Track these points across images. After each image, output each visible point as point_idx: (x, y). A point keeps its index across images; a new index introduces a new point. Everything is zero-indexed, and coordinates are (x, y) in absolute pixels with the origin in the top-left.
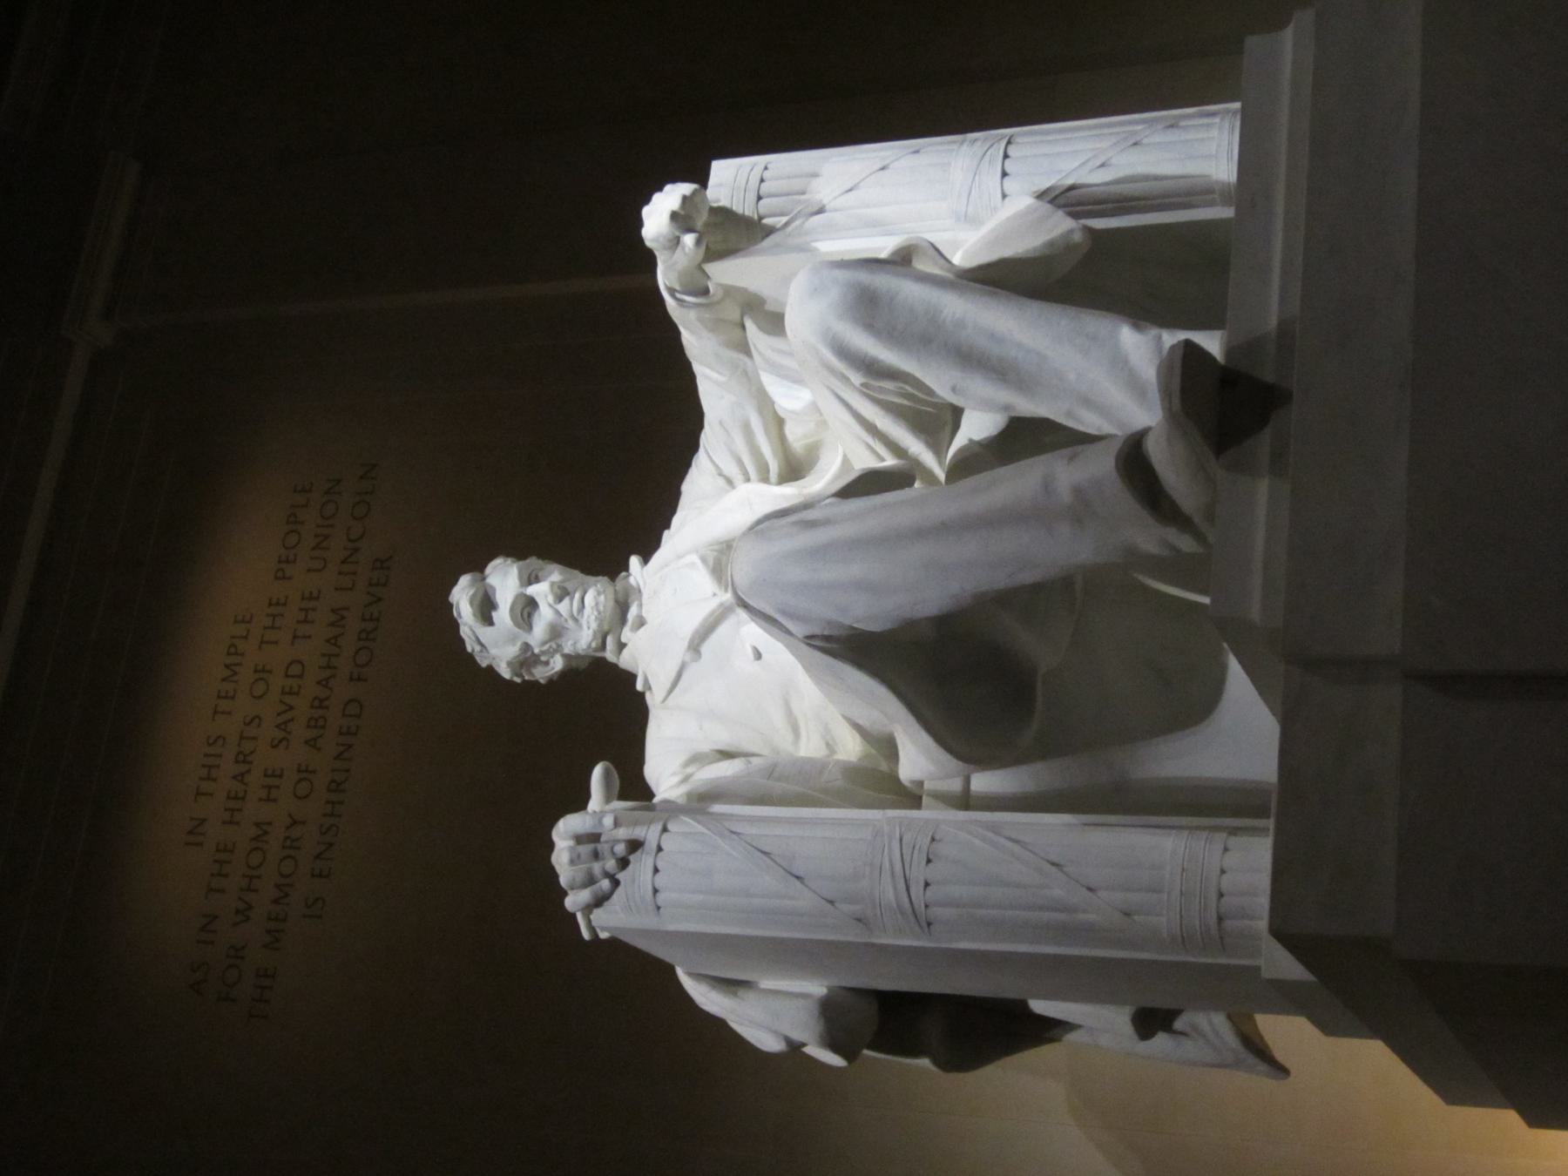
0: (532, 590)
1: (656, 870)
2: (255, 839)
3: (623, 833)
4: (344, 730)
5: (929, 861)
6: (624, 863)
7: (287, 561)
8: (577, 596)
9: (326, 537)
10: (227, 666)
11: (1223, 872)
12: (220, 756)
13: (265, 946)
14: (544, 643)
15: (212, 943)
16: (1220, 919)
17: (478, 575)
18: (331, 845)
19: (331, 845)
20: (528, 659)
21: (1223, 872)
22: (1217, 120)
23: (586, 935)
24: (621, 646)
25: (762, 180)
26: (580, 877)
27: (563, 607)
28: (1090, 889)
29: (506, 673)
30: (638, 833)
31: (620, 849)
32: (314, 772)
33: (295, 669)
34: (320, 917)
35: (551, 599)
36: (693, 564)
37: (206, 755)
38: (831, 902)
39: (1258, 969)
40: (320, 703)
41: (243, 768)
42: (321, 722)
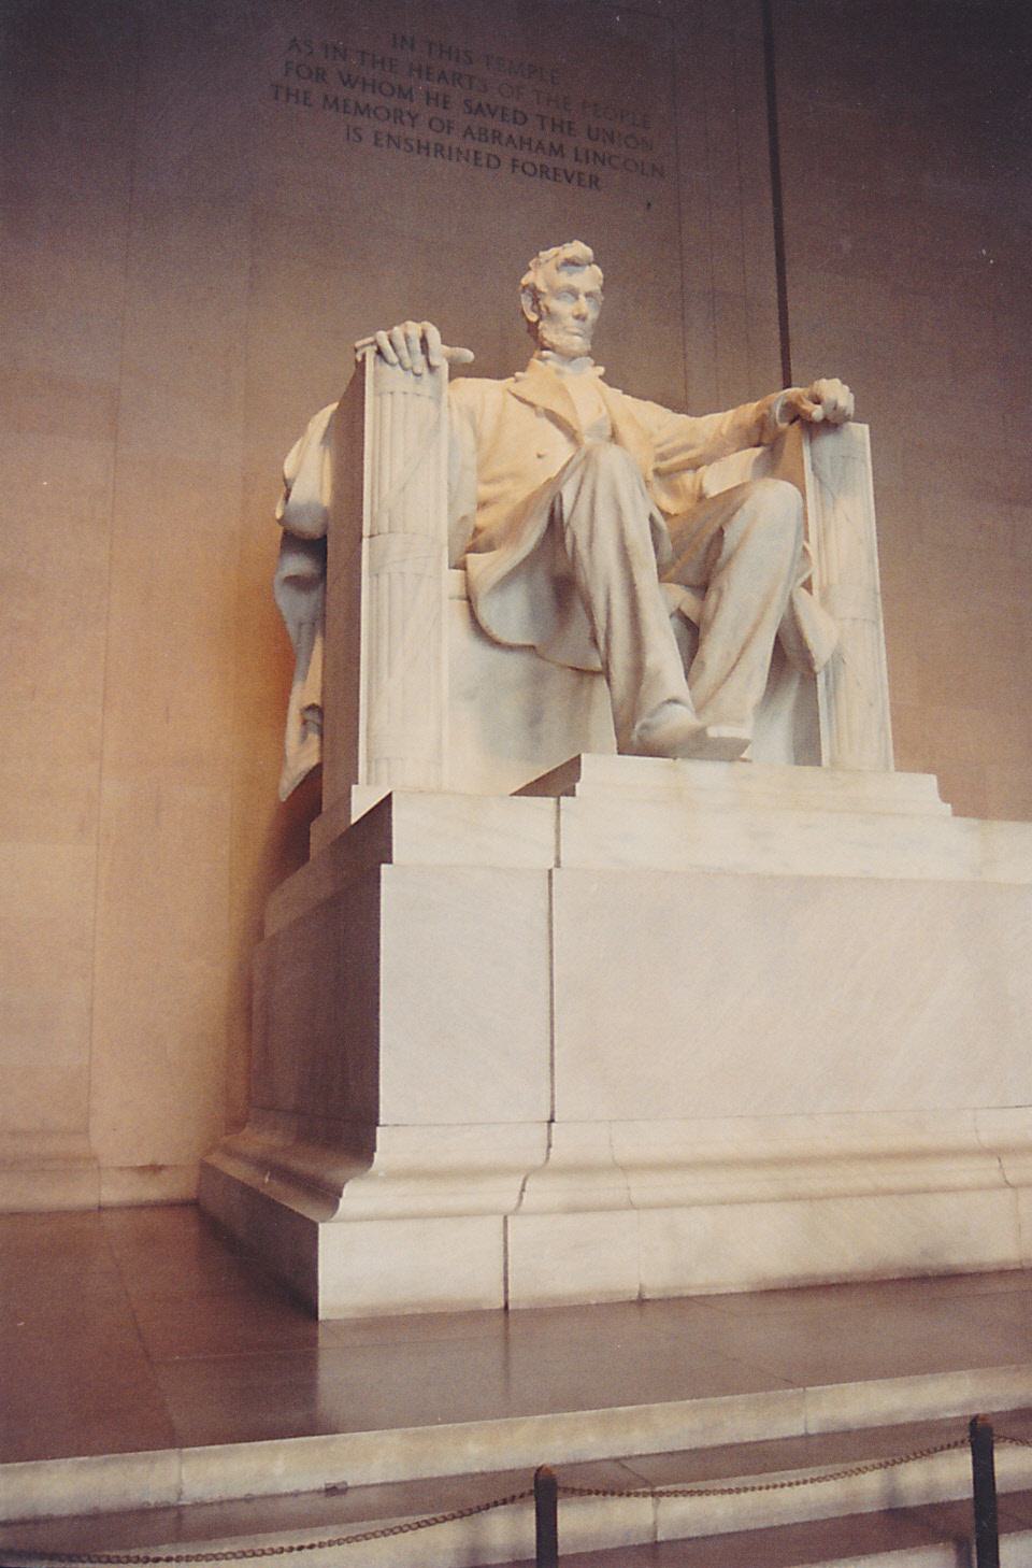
2: (400, 88)
14: (547, 309)
17: (592, 259)
19: (399, 147)
20: (535, 294)
23: (358, 344)
24: (542, 359)
27: (571, 322)
29: (527, 279)
31: (418, 370)
35: (576, 313)
36: (600, 410)
39: (357, 783)
42: (483, 137)
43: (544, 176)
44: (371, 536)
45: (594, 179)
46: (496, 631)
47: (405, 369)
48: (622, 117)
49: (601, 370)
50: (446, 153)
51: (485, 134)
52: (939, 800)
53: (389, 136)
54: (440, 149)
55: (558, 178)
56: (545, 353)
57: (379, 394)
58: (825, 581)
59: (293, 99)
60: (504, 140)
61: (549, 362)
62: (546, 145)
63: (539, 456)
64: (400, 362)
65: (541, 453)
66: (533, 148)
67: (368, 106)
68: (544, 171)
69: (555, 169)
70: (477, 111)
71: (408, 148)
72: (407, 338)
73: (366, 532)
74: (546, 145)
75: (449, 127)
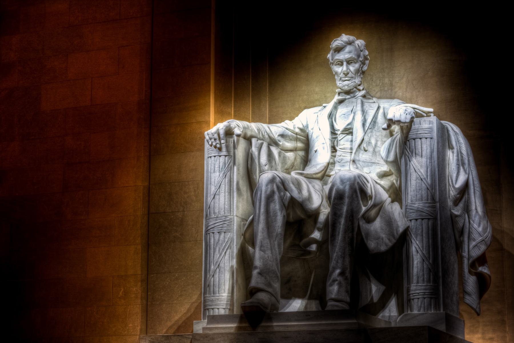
0: (345, 63)
1: (215, 156)
3: (223, 146)
5: (219, 232)
6: (215, 147)
8: (347, 79)
11: (218, 309)
16: (208, 309)
21: (218, 309)
25: (420, 139)
26: (211, 136)
27: (342, 75)
28: (213, 276)
30: (224, 149)
31: (218, 146)
38: (209, 207)
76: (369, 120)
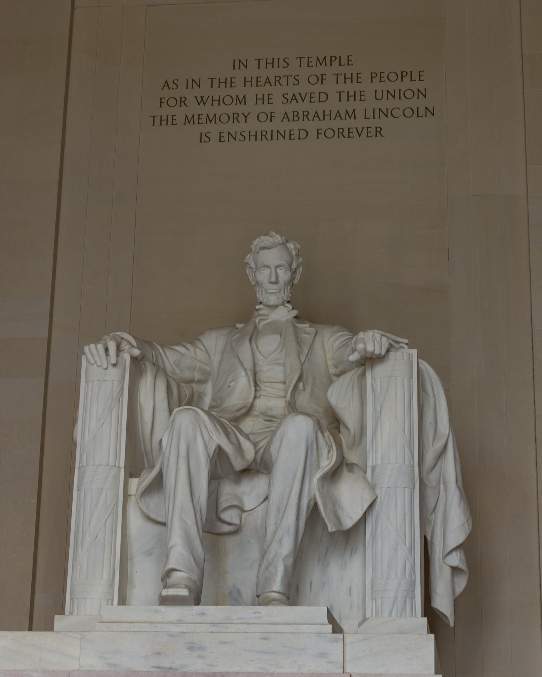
2: (237, 97)
4: (292, 132)
7: (381, 77)
9: (394, 97)
10: (325, 58)
12: (278, 67)
13: (186, 116)
15: (187, 88)
18: (235, 139)
19: (235, 139)
22: (407, 577)
31: (105, 366)
32: (271, 121)
33: (323, 97)
34: (201, 142)
37: (279, 59)
40: (306, 115)
41: (273, 82)
42: (296, 118)
43: (340, 135)
44: (79, 468)
45: (379, 130)
46: (152, 516)
47: (98, 367)
48: (402, 77)
49: (295, 313)
50: (269, 136)
51: (297, 116)
52: (327, 622)
53: (229, 133)
54: (263, 135)
55: (351, 135)
56: (257, 307)
57: (87, 382)
58: (374, 464)
59: (164, 123)
60: (311, 117)
61: (262, 312)
62: (343, 115)
63: (229, 387)
64: (95, 362)
65: (230, 385)
66: (333, 118)
67: (215, 115)
68: (340, 133)
69: (349, 129)
70: (292, 99)
71: (243, 138)
72: (97, 349)
73: (77, 465)
74: (343, 115)
75: (271, 117)
76: (306, 350)
